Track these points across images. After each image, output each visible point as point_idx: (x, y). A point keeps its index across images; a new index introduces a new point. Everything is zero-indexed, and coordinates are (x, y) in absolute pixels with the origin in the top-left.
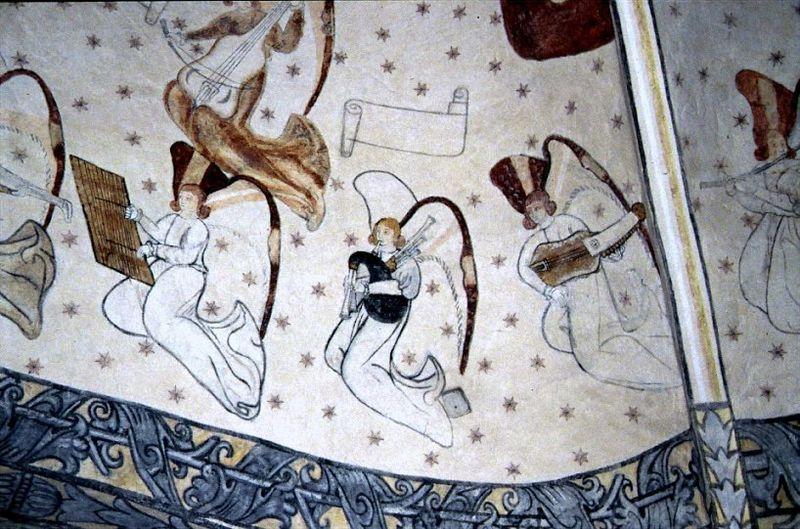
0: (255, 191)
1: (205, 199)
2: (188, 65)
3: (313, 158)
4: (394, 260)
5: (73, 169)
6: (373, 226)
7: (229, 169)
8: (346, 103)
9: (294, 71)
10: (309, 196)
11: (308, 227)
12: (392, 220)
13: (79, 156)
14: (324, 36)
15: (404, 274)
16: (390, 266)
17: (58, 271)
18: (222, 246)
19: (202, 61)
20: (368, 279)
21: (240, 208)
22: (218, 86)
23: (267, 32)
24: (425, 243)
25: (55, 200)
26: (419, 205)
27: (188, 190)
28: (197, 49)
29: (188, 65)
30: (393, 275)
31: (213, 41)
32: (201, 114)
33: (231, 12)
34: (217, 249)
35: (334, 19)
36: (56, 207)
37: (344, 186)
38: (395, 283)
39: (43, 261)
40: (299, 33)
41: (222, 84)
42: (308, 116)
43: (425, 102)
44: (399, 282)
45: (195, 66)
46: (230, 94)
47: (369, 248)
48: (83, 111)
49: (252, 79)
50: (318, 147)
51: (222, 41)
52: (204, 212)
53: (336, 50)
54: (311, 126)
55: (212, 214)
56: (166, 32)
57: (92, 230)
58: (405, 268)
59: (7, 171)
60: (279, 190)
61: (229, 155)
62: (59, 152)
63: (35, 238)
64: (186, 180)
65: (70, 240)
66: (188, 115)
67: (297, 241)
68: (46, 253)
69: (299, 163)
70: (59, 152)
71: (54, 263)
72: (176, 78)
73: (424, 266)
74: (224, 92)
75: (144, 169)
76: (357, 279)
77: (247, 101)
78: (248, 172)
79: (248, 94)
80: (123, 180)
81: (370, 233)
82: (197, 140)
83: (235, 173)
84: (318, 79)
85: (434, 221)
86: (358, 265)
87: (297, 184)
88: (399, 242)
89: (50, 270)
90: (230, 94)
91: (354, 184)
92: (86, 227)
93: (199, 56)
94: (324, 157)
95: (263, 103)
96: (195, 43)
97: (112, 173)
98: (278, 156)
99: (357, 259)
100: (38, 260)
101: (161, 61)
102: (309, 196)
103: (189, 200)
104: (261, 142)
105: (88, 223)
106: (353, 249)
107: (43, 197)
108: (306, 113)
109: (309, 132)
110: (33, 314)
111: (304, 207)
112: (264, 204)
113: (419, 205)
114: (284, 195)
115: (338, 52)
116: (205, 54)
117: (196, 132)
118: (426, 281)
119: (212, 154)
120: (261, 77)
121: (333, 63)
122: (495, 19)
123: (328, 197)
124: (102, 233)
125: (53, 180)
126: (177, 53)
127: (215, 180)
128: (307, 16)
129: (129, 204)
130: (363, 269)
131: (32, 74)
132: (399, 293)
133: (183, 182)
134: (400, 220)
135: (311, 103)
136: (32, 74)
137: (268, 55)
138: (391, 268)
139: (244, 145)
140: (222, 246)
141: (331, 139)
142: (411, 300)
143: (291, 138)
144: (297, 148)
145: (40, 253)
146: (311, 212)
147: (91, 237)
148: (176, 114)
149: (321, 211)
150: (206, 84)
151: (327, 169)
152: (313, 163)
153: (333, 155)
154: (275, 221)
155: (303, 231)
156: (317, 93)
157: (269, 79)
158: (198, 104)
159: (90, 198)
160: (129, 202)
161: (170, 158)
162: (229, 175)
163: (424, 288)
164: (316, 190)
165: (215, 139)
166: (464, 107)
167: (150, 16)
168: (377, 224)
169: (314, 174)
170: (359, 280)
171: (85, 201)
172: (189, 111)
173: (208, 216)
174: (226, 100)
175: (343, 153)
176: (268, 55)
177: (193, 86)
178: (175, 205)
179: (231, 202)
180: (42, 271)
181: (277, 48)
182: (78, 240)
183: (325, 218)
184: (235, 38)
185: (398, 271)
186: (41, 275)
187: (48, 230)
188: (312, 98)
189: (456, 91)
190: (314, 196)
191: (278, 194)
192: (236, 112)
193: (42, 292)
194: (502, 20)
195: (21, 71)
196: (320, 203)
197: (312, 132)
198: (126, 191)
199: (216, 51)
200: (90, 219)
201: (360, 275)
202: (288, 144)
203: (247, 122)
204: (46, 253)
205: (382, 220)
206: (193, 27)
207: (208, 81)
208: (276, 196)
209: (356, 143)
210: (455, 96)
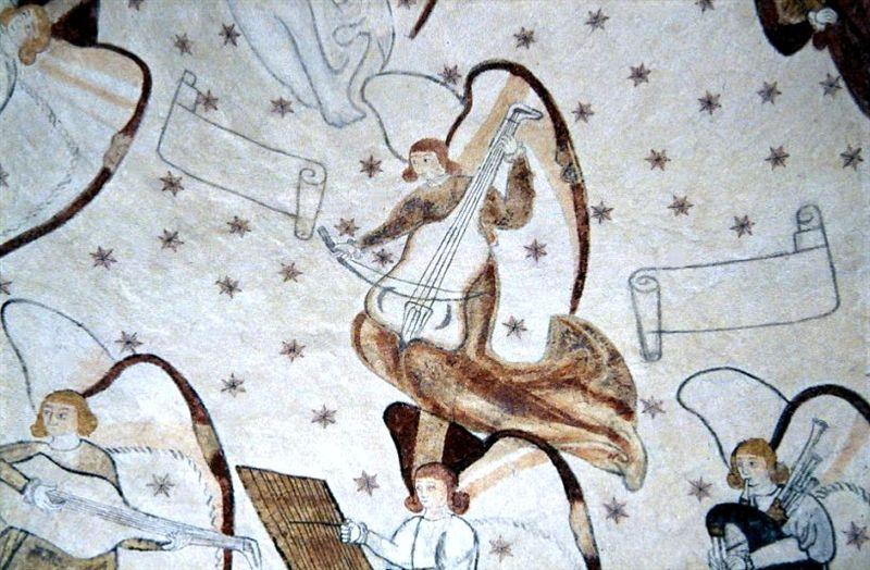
0: (529, 450)
1: (456, 482)
2: (376, 285)
3: (604, 377)
4: (779, 505)
5: (246, 487)
6: (728, 458)
7: (479, 426)
8: (631, 278)
9: (536, 251)
10: (613, 436)
11: (627, 486)
12: (755, 441)
14: (567, 186)
15: (803, 523)
16: (776, 515)
18: (502, 549)
19: (394, 274)
20: (745, 546)
21: (511, 483)
22: (428, 304)
23: (481, 204)
24: (820, 465)
25: (229, 542)
26: (792, 407)
27: (425, 475)
28: (383, 258)
29: (376, 285)
30: (785, 529)
31: (403, 239)
32: (414, 352)
33: (418, 189)
34: (496, 557)
35: (576, 158)
36: (234, 553)
37: (664, 407)
38: (792, 544)
40: (528, 193)
41: (434, 299)
42: (577, 314)
43: (755, 243)
44: (797, 538)
45: (384, 284)
46: (449, 311)
47: (733, 495)
48: (239, 394)
49: (478, 280)
50: (605, 357)
51: (417, 235)
52: (460, 503)
53: (592, 202)
54: (587, 327)
55: (473, 503)
56: (330, 245)
58: (801, 512)
59: (148, 515)
60: (566, 439)
61: (474, 405)
62: (218, 465)
64: (419, 460)
66: (396, 360)
67: (616, 512)
69: (584, 388)
70: (218, 465)
72: (363, 308)
73: (831, 501)
74: (440, 310)
75: (352, 457)
76: (728, 550)
77: (479, 316)
78: (512, 423)
79: (477, 304)
80: (325, 485)
81: (727, 471)
82: (420, 394)
83: (489, 429)
84: (578, 253)
85: (824, 426)
86: (723, 528)
87: (593, 423)
88: (779, 475)
90: (449, 311)
91: (679, 400)
93: (389, 266)
94: (621, 370)
95: (503, 313)
96: (377, 249)
97: (305, 478)
98: (549, 387)
99: (718, 518)
101: (337, 290)
102: (613, 436)
103: (432, 489)
104: (517, 372)
106: (708, 504)
107: (211, 542)
108: (573, 310)
109: (585, 338)
111: (611, 456)
112: (549, 468)
113: (792, 407)
114: (574, 445)
115: (596, 204)
116: (396, 262)
117: (415, 380)
118: (842, 525)
119: (448, 410)
120: (490, 273)
121: (593, 222)
122: (830, 87)
123: (644, 430)
125: (219, 511)
126: (354, 271)
127: (463, 449)
128: (534, 164)
130: (734, 532)
131: (151, 358)
132: (803, 556)
133: (417, 464)
134: (768, 438)
135: (577, 293)
136: (151, 358)
137: (490, 239)
138: (778, 518)
139: (493, 382)
140: (502, 549)
141: (622, 338)
142: (827, 563)
143: (560, 354)
144: (575, 366)
146: (624, 460)
148: (379, 364)
149: (640, 456)
150: (410, 305)
151: (631, 387)
152: (606, 384)
153: (635, 367)
154: (573, 490)
155: (622, 495)
156: (581, 276)
157: (503, 272)
158: (407, 338)
159: (282, 525)
160: (342, 515)
161: (385, 432)
162: (482, 436)
163: (842, 539)
164: (621, 424)
165: (447, 385)
166: (819, 233)
167: (300, 228)
168: (734, 453)
169: (611, 400)
170: (732, 552)
171: (275, 532)
172: (396, 352)
173: (467, 507)
174: (447, 321)
175: (648, 357)
176: (490, 239)
177: (393, 314)
178: (414, 502)
179: (498, 475)
181: (502, 223)
183: (650, 467)
184: (435, 225)
185: (792, 520)
188: (577, 284)
189: (798, 213)
190: (622, 435)
191: (564, 445)
192: (467, 336)
194: (842, 83)
195: (136, 358)
196: (635, 444)
197: (590, 337)
198: (334, 500)
199: (411, 255)
200: (290, 559)
201: (732, 543)
202: (561, 364)
203: (487, 345)
205: (740, 445)
206: (369, 227)
207: (410, 301)
208: (564, 449)
209: (664, 336)
210: (799, 222)
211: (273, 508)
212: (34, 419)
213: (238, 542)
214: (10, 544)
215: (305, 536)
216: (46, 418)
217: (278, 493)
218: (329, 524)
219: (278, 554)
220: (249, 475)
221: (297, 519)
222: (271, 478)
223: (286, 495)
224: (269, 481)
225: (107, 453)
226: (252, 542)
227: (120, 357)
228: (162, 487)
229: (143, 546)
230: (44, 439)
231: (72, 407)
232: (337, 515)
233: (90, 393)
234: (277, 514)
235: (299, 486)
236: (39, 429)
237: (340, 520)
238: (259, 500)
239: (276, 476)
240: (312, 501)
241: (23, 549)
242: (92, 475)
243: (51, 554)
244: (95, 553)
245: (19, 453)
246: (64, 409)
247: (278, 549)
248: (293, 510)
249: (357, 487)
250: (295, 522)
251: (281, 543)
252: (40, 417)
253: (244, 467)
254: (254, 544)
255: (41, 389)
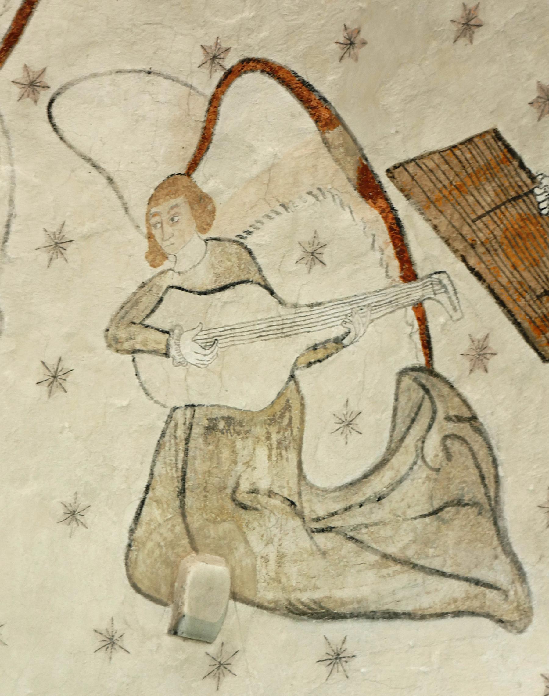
5: (408, 197)
13: (402, 157)
17: (493, 442)
25: (415, 291)
36: (427, 305)
39: (463, 440)
57: (504, 297)
59: (311, 305)
62: (368, 185)
63: (427, 404)
65: (480, 355)
68: (459, 419)
71: (479, 430)
80: (497, 136)
89: (482, 453)
92: (491, 300)
97: (470, 140)
100: (455, 446)
105: (492, 291)
107: (394, 304)
110: (500, 573)
124: (523, 288)
129: (533, 178)
136: (247, 64)
145: (451, 428)
147: (510, 314)
159: (466, 230)
160: (529, 173)
171: (460, 245)
180: (470, 462)
182: (492, 344)
186: (474, 475)
187: (438, 367)
193: (493, 510)
195: (230, 75)
204: (459, 419)
211: (448, 210)
212: (145, 244)
213: (425, 286)
214: (181, 433)
215: (498, 233)
216: (157, 233)
217: (446, 183)
218: (519, 197)
219: (473, 279)
220: (404, 177)
221: (480, 212)
222: (431, 165)
223: (457, 181)
224: (431, 171)
225: (239, 242)
226: (442, 276)
227: (210, 91)
228: (314, 255)
229: (320, 354)
230: (167, 264)
231: (180, 200)
232: (524, 175)
233: (193, 165)
234: (456, 216)
235: (469, 156)
236: (156, 254)
237: (529, 181)
238: (428, 207)
239: (436, 157)
240: (489, 171)
241: (197, 430)
242: (233, 285)
243: (229, 420)
244: (273, 396)
245: (148, 301)
246: (172, 208)
247: (472, 270)
248: (471, 199)
249: (537, 115)
250: (479, 217)
251: (472, 261)
252: (150, 237)
253: (395, 167)
254: (445, 281)
255: (138, 195)
